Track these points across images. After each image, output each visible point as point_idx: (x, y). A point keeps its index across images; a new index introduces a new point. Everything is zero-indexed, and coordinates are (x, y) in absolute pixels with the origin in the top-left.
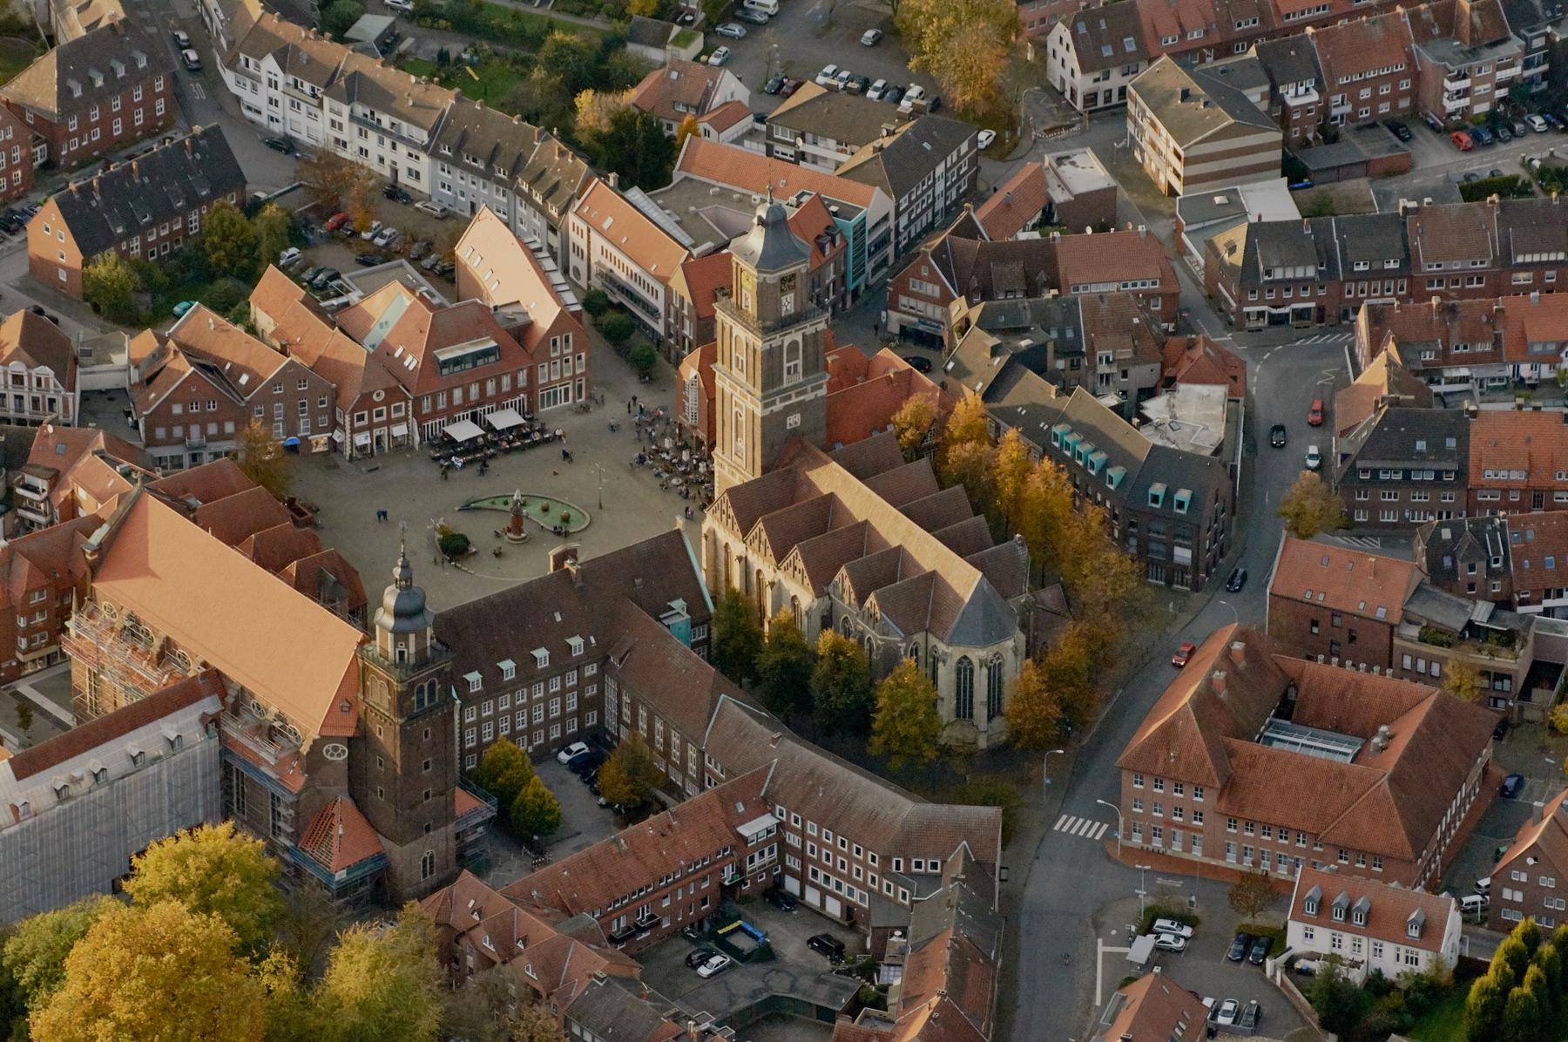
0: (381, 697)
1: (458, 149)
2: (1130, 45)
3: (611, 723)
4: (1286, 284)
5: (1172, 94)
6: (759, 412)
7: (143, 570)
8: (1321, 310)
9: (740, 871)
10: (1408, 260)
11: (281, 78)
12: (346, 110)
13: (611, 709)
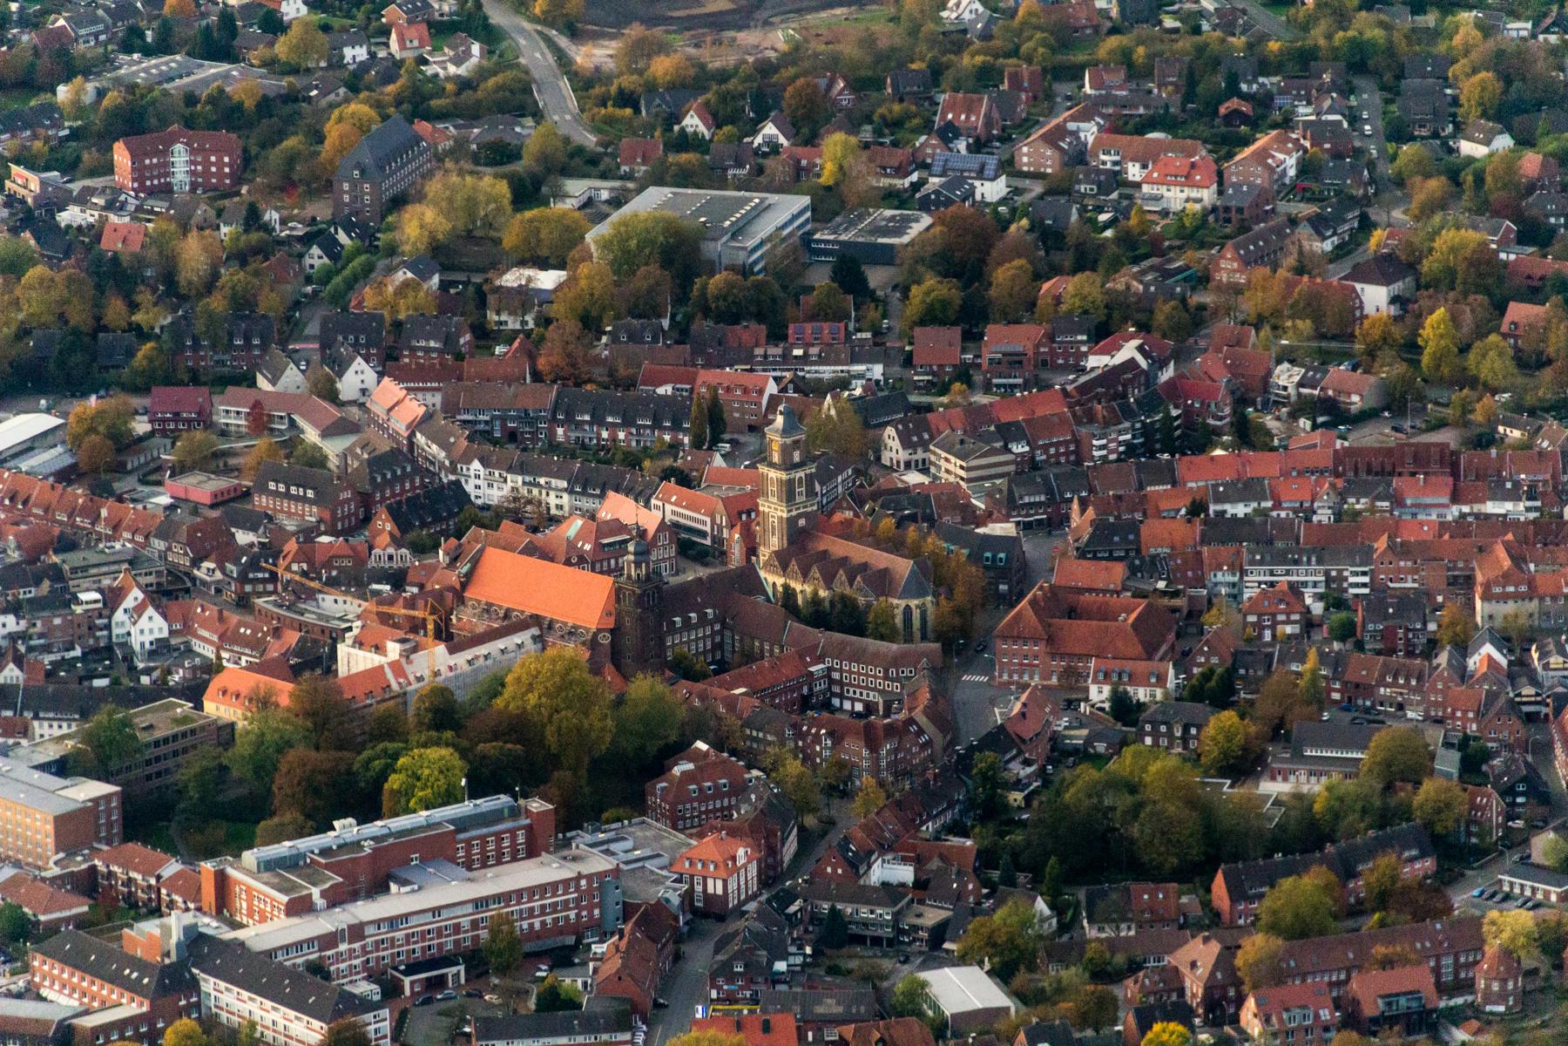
0: (627, 605)
1: (584, 488)
2: (926, 436)
3: (728, 655)
4: (1030, 505)
8: (1049, 519)
9: (810, 689)
11: (482, 471)
12: (520, 479)
13: (728, 648)
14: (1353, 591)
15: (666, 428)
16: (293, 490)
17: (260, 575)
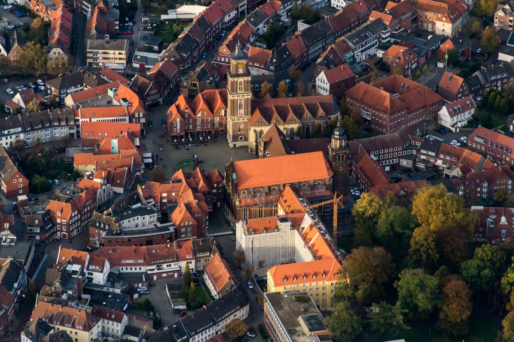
5: (103, 45)
6: (250, 97)
7: (248, 177)
10: (197, 42)
17: (49, 226)
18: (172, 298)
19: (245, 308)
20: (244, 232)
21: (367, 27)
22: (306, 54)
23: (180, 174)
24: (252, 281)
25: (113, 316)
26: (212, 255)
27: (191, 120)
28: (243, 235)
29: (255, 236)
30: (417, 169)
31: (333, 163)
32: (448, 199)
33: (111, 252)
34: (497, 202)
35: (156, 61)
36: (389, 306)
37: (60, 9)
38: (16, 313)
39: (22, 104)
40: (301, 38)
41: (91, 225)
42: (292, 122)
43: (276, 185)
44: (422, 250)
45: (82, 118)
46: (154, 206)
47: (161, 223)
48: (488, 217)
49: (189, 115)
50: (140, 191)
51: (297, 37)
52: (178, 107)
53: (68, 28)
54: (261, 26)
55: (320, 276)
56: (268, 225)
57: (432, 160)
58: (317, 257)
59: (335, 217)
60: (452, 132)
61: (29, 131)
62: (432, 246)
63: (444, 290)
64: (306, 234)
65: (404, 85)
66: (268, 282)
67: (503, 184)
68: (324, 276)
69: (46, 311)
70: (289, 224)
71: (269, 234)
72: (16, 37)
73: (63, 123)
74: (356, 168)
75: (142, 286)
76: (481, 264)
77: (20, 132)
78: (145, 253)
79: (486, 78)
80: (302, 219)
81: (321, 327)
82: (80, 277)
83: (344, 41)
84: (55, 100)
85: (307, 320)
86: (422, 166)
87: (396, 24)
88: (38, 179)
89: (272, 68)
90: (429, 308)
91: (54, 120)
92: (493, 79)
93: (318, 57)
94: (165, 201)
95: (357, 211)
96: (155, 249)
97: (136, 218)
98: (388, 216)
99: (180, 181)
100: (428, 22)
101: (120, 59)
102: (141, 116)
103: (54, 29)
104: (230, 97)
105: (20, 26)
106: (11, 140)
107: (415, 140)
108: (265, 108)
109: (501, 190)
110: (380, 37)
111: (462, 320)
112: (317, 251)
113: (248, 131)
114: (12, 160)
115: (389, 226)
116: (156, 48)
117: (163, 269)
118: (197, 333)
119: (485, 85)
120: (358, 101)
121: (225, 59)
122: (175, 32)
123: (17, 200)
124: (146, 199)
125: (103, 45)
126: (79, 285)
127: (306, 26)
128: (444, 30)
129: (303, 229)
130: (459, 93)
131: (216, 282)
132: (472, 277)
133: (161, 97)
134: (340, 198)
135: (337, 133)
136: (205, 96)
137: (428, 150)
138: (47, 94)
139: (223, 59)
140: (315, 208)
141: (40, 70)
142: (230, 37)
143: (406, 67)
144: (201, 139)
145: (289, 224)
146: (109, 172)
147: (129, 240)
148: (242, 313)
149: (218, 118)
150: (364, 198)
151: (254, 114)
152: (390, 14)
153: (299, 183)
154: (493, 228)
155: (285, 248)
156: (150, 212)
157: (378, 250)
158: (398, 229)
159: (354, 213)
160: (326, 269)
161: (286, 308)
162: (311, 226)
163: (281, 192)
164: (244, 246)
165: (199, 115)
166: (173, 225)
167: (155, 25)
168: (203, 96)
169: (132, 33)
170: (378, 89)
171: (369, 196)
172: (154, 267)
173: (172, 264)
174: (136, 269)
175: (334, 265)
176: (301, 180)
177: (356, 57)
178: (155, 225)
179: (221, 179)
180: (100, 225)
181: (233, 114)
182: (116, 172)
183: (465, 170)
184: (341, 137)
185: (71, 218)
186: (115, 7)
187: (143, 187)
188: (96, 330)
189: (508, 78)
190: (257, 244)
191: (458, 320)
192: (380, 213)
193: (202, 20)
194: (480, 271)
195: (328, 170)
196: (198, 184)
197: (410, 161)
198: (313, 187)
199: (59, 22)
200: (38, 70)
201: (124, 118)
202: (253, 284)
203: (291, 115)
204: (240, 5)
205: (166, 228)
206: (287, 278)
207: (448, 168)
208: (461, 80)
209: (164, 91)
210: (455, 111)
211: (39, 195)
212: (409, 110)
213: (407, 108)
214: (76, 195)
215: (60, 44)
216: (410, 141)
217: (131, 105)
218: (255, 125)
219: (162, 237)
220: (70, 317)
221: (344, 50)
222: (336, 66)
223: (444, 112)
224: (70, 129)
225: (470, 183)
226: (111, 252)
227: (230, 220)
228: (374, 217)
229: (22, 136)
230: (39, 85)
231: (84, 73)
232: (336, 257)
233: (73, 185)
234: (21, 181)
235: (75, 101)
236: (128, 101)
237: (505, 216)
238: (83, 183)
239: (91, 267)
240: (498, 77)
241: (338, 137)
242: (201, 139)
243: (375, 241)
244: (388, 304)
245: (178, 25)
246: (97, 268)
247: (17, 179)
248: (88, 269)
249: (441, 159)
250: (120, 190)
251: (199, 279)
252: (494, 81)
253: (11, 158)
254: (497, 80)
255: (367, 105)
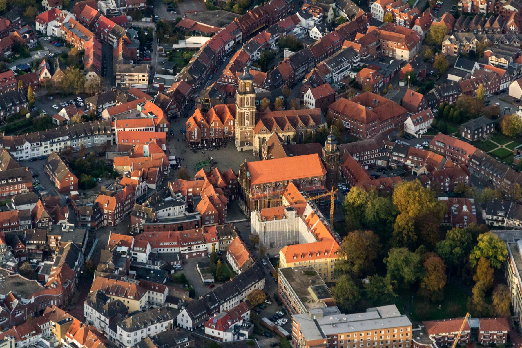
6: (255, 110)
7: (259, 175)
10: (205, 67)
12: (49, 142)
14: (355, 65)
15: (18, 104)
16: (10, 181)
18: (202, 273)
19: (262, 281)
20: (258, 220)
21: (341, 53)
22: (293, 76)
23: (202, 173)
24: (266, 259)
25: (157, 288)
26: (232, 238)
27: (206, 129)
28: (258, 222)
29: (267, 222)
30: (390, 168)
31: (327, 163)
32: (422, 192)
33: (151, 236)
34: (457, 194)
35: (172, 82)
36: (381, 278)
37: (92, 39)
38: (76, 286)
39: (67, 117)
40: (289, 63)
41: (132, 215)
42: (289, 130)
43: (281, 182)
44: (403, 232)
45: (117, 128)
46: (182, 198)
47: (189, 212)
48: (452, 206)
49: (204, 125)
50: (171, 187)
51: (286, 62)
52: (195, 119)
53: (99, 56)
54: (255, 53)
55: (322, 254)
56: (278, 214)
57: (402, 161)
58: (319, 239)
59: (332, 207)
60: (416, 138)
61: (75, 139)
62: (412, 230)
63: (425, 264)
64: (309, 220)
65: (376, 101)
66: (281, 259)
67: (462, 179)
68: (326, 254)
69: (104, 284)
70: (294, 212)
71: (278, 221)
72: (58, 63)
73: (102, 133)
74: (342, 167)
75: (177, 263)
76: (453, 243)
77: (68, 140)
78: (179, 237)
79: (440, 94)
80: (304, 209)
81: (327, 295)
82: (128, 257)
83: (324, 65)
84: (94, 113)
85: (316, 290)
86: (394, 165)
87: (364, 52)
88: (86, 178)
89: (267, 87)
90: (413, 279)
91: (95, 130)
92: (445, 95)
93: (304, 78)
94: (190, 194)
95: (348, 202)
96: (186, 233)
97: (168, 208)
98: (374, 205)
99: (202, 178)
100: (390, 49)
101: (143, 80)
102: (165, 126)
103: (88, 56)
104: (238, 110)
105: (59, 54)
106: (61, 146)
107: (389, 144)
108: (266, 119)
109: (460, 184)
110: (352, 61)
111: (439, 289)
112: (319, 234)
113: (253, 137)
114: (64, 162)
115: (375, 214)
116: (171, 71)
117: (193, 250)
118: (226, 301)
119: (439, 100)
120: (340, 113)
121: (228, 80)
122: (185, 58)
123: (70, 194)
124: (176, 193)
125: (129, 69)
126: (127, 263)
127: (292, 53)
128: (402, 56)
129: (306, 216)
130: (419, 106)
131: (237, 260)
132: (446, 254)
133: (179, 111)
134: (336, 191)
135: (330, 139)
136: (217, 110)
137: (399, 152)
138: (86, 109)
139: (226, 80)
140: (316, 200)
141: (79, 89)
142: (232, 62)
143: (375, 86)
144: (214, 144)
145: (294, 212)
146: (144, 172)
147: (164, 226)
148: (260, 285)
149: (228, 127)
150: (353, 191)
151: (258, 124)
152: (359, 43)
153: (300, 179)
154: (456, 215)
155: (291, 232)
156: (180, 204)
157: (368, 233)
158: (382, 216)
159: (345, 203)
160: (327, 249)
161: (297, 280)
162: (313, 214)
163: (285, 187)
164: (258, 230)
165: (213, 125)
166: (199, 214)
167: (168, 53)
168: (215, 110)
169: (150, 59)
170: (356, 103)
171: (357, 189)
172: (186, 248)
173: (201, 246)
174: (171, 250)
175: (333, 245)
176: (302, 177)
177: (334, 78)
178: (185, 214)
179: (235, 177)
180: (140, 214)
181: (241, 123)
182: (150, 171)
183: (430, 168)
184: (334, 142)
185: (116, 209)
186: (135, 38)
187: (173, 183)
188: (144, 299)
189: (457, 94)
190: (268, 229)
191: (436, 289)
192: (366, 203)
193: (208, 48)
194: (452, 249)
195: (323, 168)
196: (217, 181)
197: (384, 161)
198: (311, 183)
199: (92, 50)
200: (77, 89)
201: (151, 128)
202: (266, 261)
203: (288, 125)
204: (237, 36)
205: (194, 217)
206: (296, 256)
207: (416, 167)
208: (421, 96)
209: (181, 106)
210: (417, 121)
211: (86, 190)
212: (381, 120)
213: (379, 119)
214: (119, 190)
215: (94, 68)
216: (384, 145)
217: (156, 117)
218: (259, 133)
219: (191, 224)
220: (123, 289)
221: (324, 72)
222: (318, 85)
223: (409, 122)
224: (107, 137)
225: (435, 178)
226: (151, 236)
227: (243, 209)
228: (363, 206)
229: (69, 143)
230: (79, 102)
231: (116, 91)
232: (335, 238)
233: (116, 183)
234: (72, 179)
235: (110, 115)
236: (153, 114)
237: (466, 205)
238: (124, 181)
239: (135, 249)
240: (450, 94)
241: (331, 142)
242: (214, 144)
243: (364, 226)
244: (379, 276)
245: (187, 53)
246: (141, 249)
247: (69, 177)
248: (133, 250)
249: (409, 159)
250: (153, 186)
251: (223, 258)
252: (447, 96)
253: (63, 160)
254: (449, 96)
255: (346, 116)
